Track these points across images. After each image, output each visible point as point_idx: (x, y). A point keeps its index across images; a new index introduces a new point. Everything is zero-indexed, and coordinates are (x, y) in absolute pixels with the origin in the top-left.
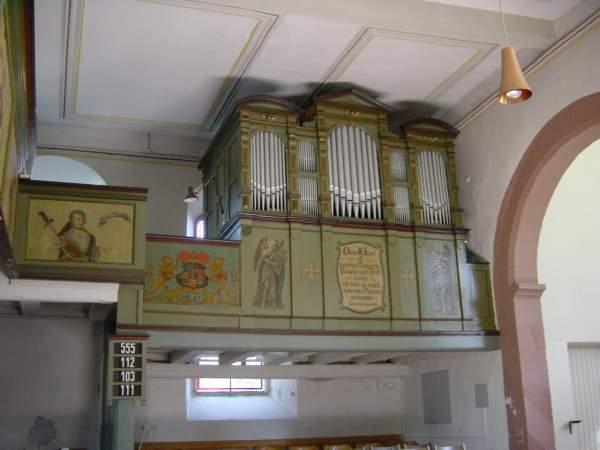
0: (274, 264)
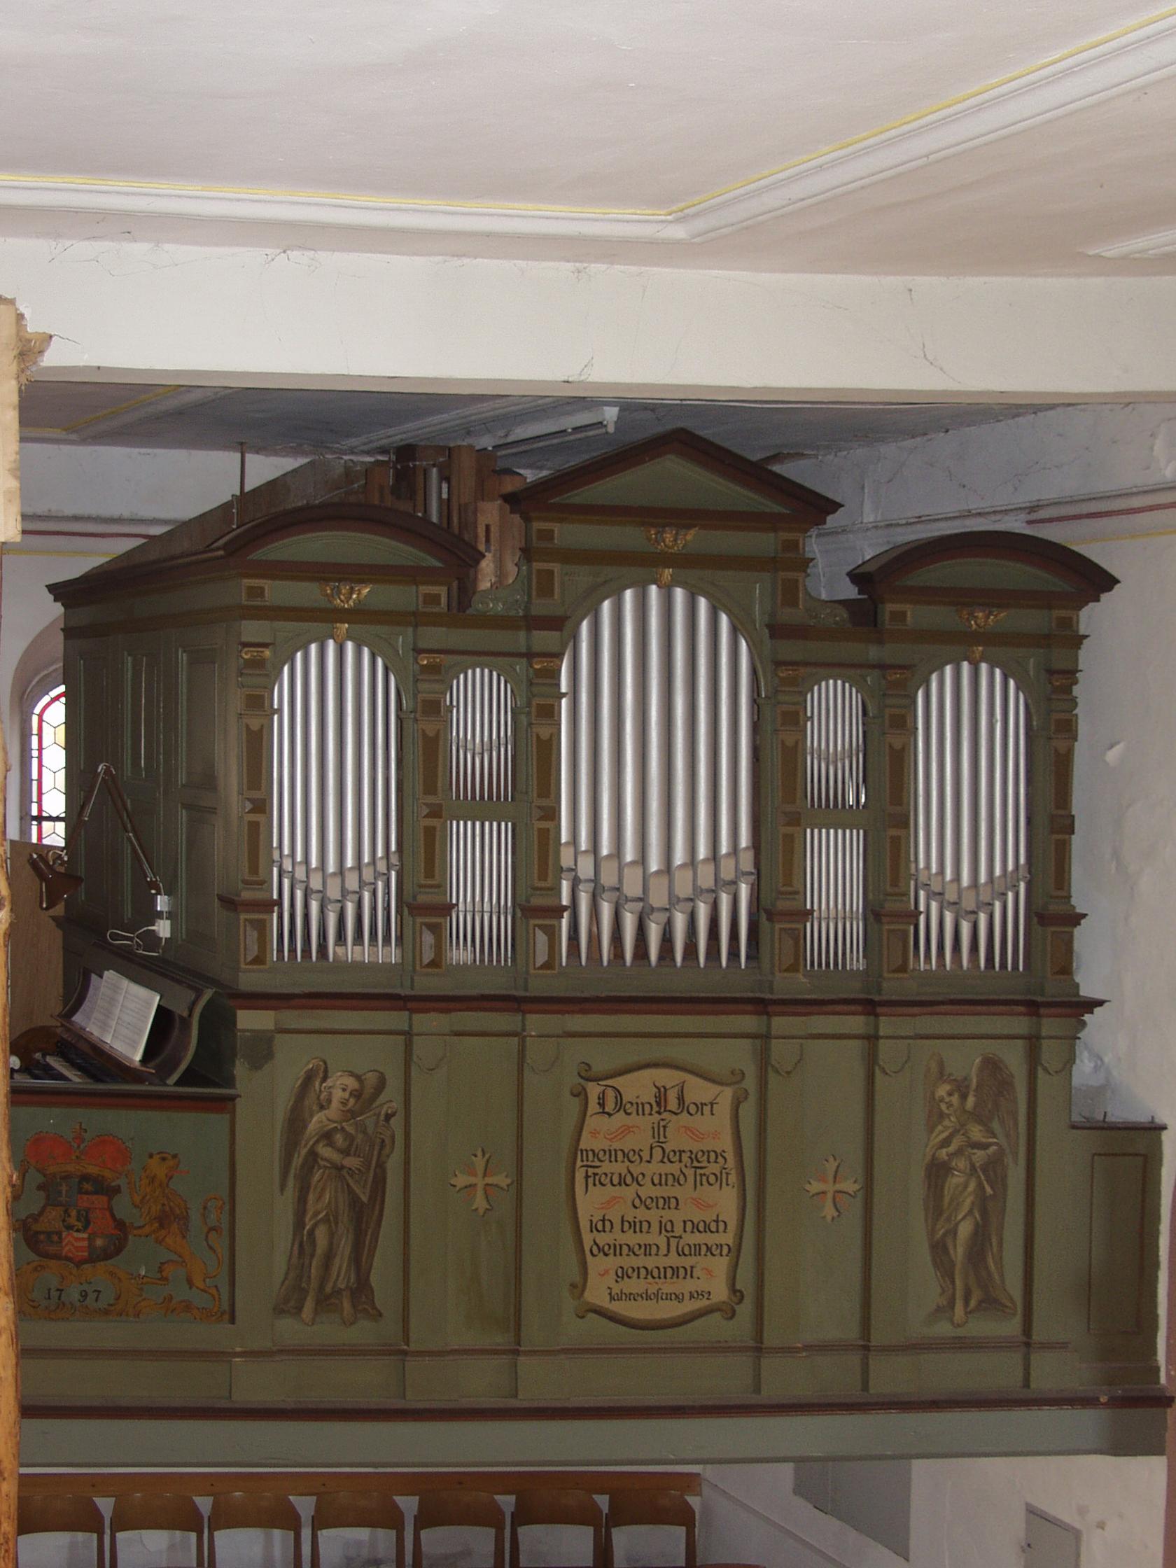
0: (352, 1162)
